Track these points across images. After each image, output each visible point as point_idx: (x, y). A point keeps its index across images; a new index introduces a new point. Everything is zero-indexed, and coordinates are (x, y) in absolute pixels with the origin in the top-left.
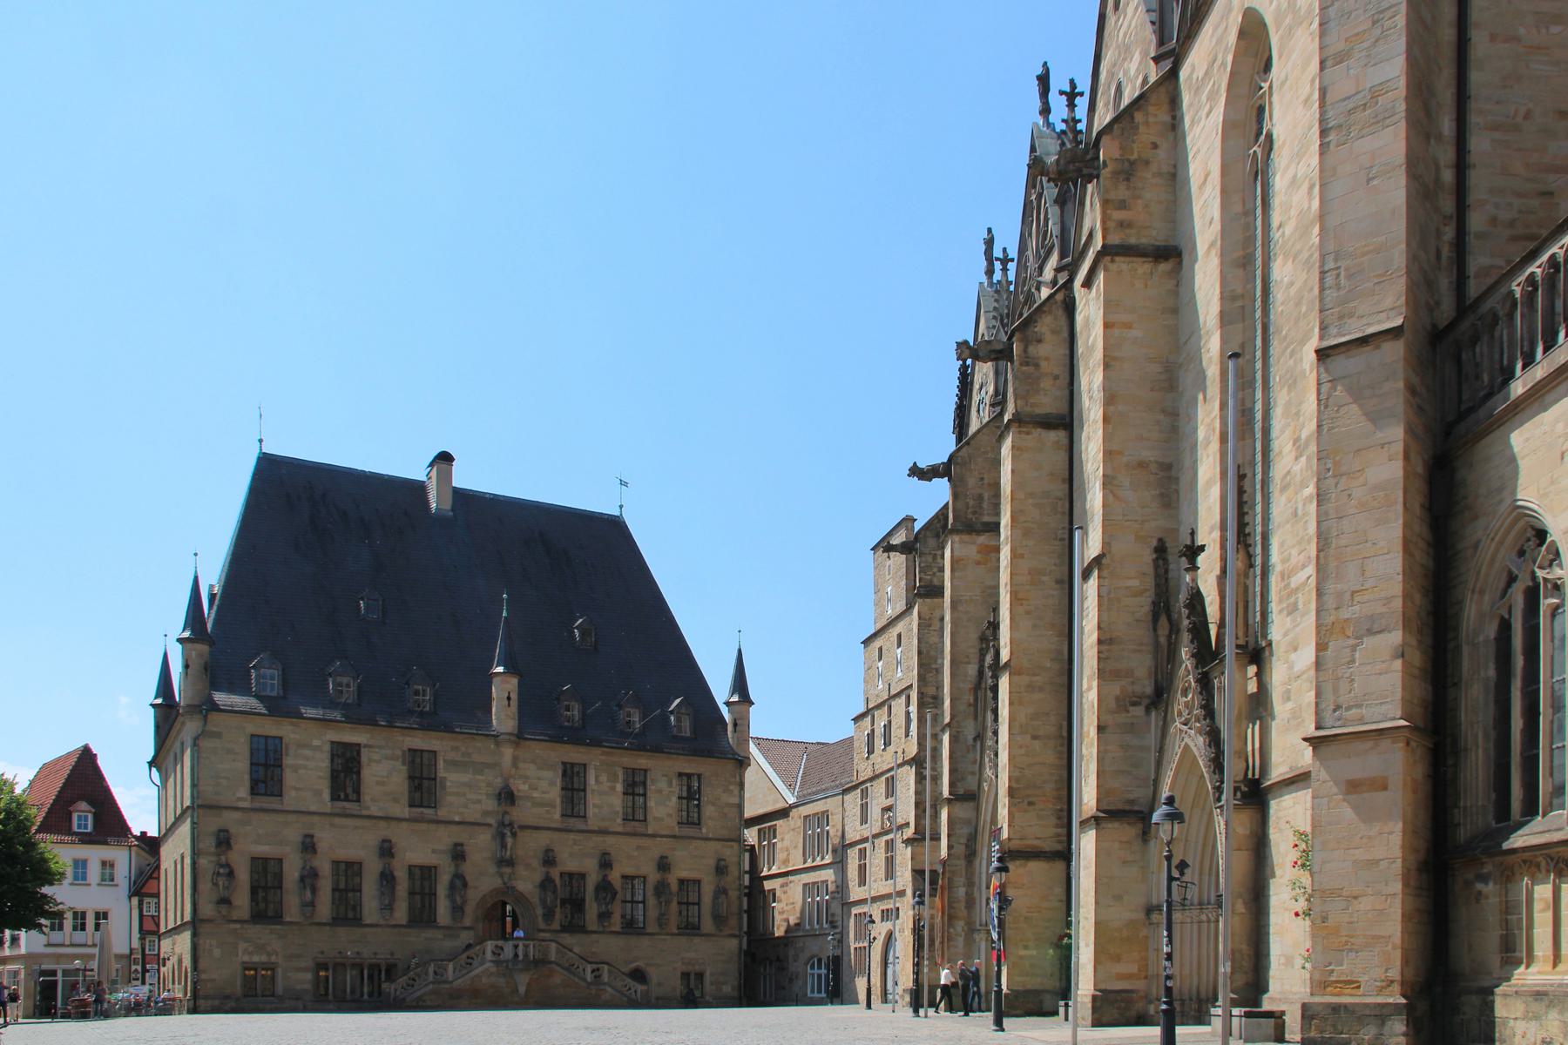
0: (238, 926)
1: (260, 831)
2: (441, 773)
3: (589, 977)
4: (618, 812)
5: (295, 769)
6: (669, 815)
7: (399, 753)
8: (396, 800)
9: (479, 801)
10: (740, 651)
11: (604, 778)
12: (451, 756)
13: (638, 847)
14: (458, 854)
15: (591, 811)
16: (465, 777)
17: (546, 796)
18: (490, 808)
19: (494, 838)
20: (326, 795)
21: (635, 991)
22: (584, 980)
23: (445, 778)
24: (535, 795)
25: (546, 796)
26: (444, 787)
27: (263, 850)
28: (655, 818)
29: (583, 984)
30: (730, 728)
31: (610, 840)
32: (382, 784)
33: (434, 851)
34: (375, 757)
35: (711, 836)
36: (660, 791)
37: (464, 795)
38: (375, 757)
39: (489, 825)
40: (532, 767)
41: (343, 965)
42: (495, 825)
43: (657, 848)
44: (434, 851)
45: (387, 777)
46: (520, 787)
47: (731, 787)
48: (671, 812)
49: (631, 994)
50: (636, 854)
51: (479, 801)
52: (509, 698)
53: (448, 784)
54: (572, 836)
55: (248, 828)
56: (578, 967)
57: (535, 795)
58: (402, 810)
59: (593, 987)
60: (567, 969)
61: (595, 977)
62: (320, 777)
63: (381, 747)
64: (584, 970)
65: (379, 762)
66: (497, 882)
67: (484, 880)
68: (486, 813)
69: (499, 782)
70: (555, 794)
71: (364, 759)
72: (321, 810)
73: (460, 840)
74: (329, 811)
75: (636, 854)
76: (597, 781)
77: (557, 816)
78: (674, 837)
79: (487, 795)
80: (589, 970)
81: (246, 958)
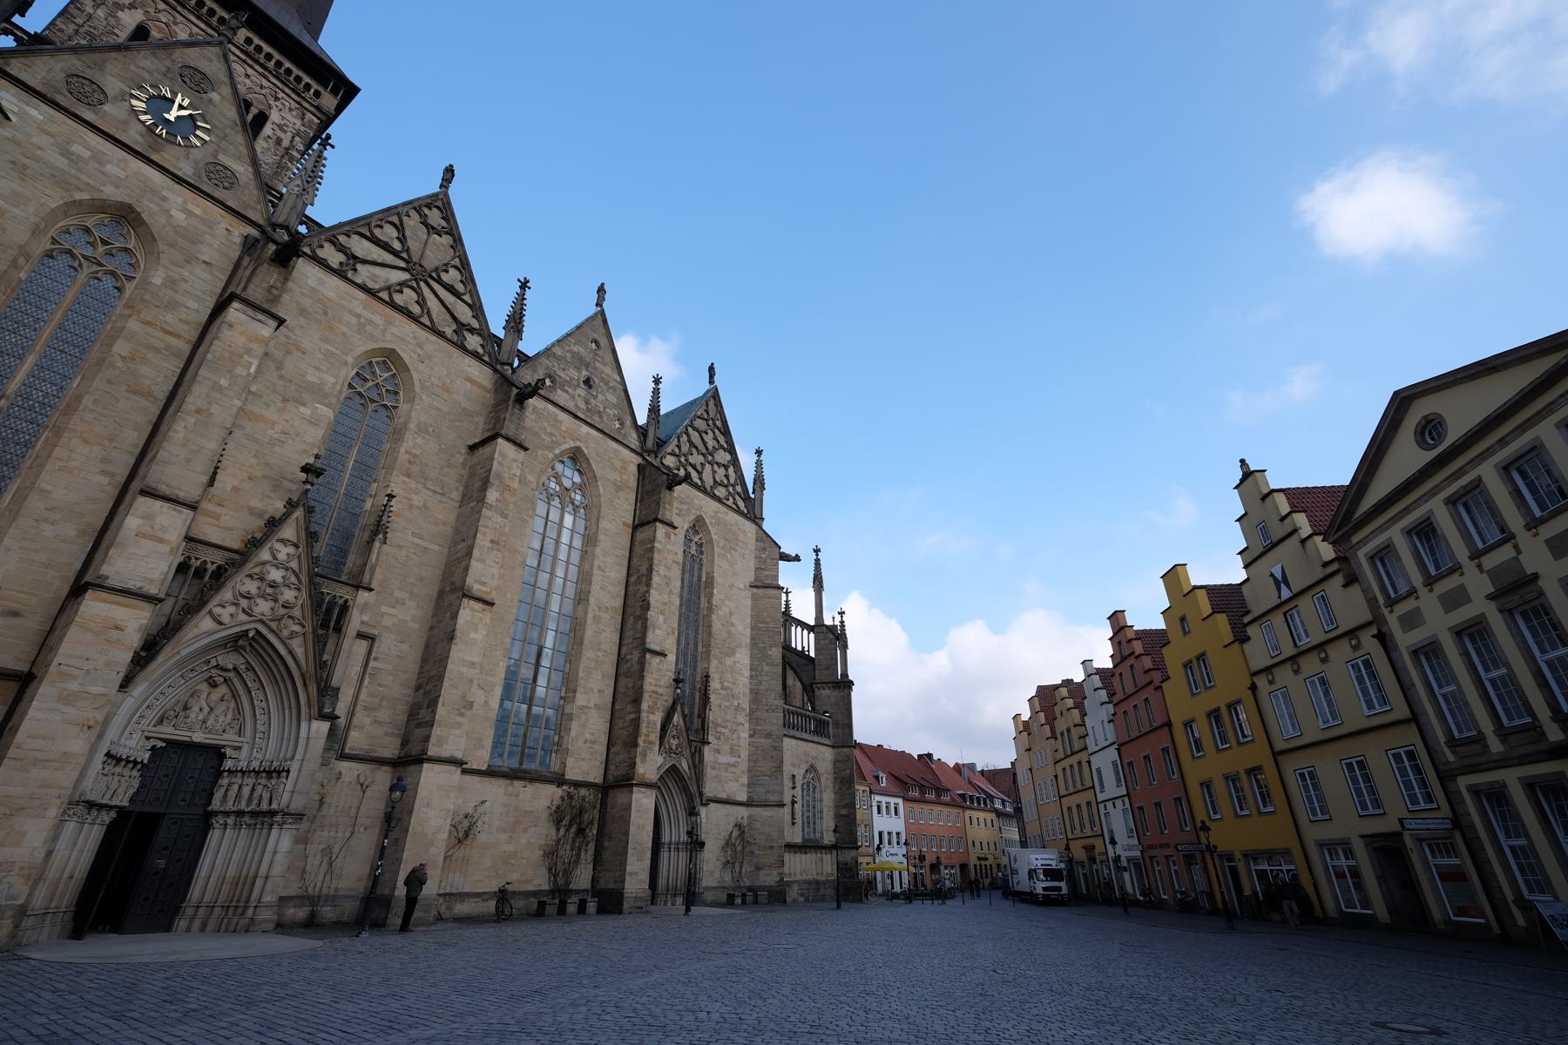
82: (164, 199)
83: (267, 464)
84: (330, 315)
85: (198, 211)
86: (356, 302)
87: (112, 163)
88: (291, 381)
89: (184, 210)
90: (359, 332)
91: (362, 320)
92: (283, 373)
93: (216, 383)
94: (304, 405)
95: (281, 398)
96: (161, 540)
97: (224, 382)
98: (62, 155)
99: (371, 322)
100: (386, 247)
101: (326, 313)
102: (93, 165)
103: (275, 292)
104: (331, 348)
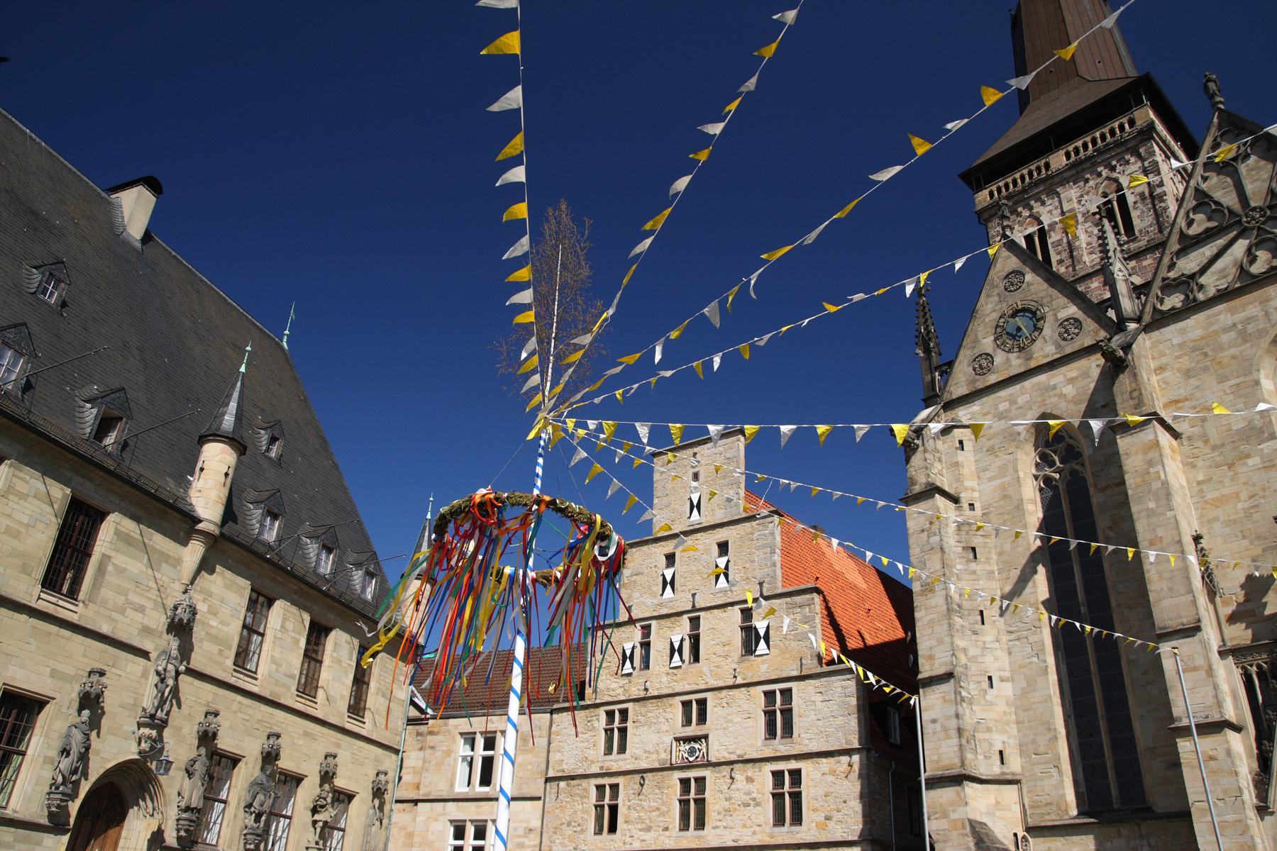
4: (292, 677)
8: (25, 570)
9: (141, 610)
11: (290, 626)
13: (306, 734)
17: (225, 629)
18: (153, 625)
19: (145, 675)
23: (109, 557)
24: (213, 623)
25: (225, 629)
26: (101, 570)
32: (17, 536)
33: (54, 674)
36: (339, 662)
37: (125, 593)
39: (144, 654)
44: (54, 674)
51: (141, 610)
52: (227, 475)
53: (110, 568)
65: (23, 496)
66: (130, 752)
68: (146, 631)
73: (99, 666)
75: (301, 742)
82: (1054, 387)
83: (1258, 538)
84: (1210, 353)
85: (1074, 374)
86: (1222, 317)
87: (1018, 396)
88: (1223, 445)
89: (1071, 381)
90: (1245, 341)
91: (1240, 327)
92: (1212, 442)
93: (1148, 509)
94: (1248, 456)
95: (1226, 467)
96: (1195, 669)
97: (1152, 505)
98: (999, 419)
99: (1249, 320)
100: (1207, 236)
101: (1206, 355)
102: (1015, 407)
103: (1135, 394)
104: (1233, 382)
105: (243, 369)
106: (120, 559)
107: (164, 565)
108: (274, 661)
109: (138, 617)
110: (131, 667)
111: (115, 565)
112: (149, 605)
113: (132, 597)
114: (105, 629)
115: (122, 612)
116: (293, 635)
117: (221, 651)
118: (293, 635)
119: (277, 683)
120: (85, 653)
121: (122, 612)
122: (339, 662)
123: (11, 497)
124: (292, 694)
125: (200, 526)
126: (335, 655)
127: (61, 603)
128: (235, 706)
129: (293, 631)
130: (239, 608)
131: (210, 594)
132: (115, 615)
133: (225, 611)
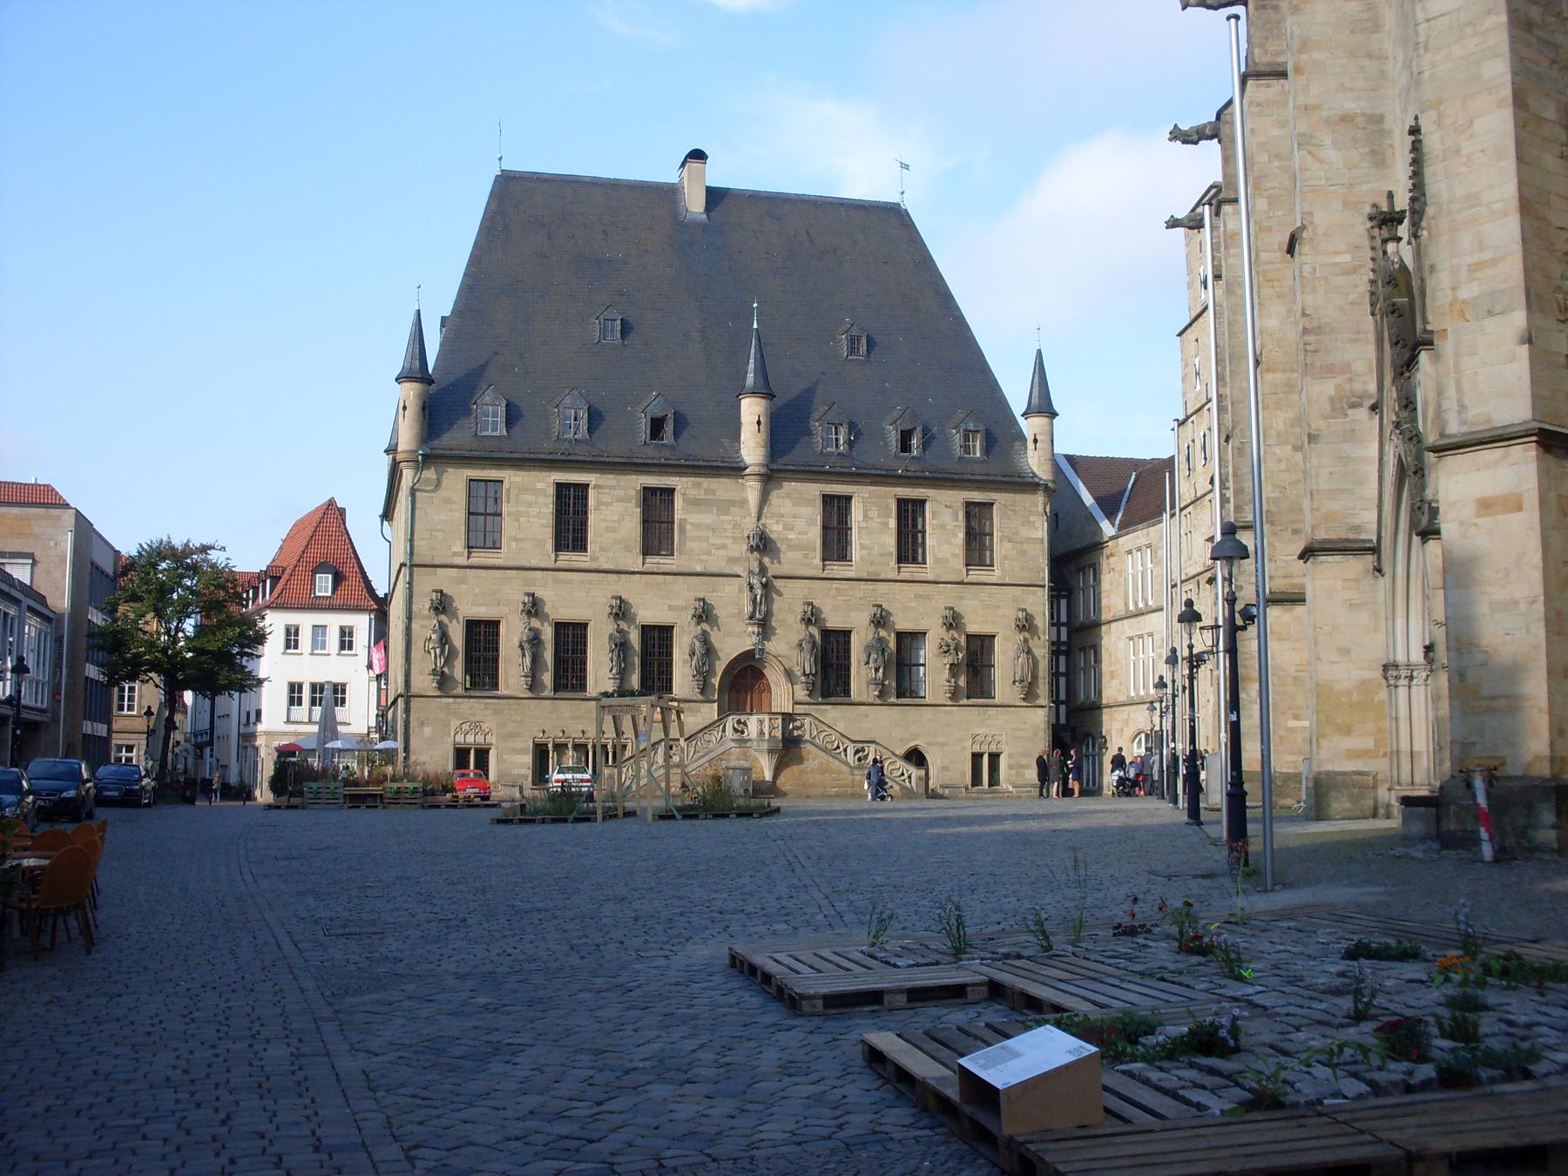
0: (451, 700)
1: (477, 591)
2: (679, 514)
3: (851, 758)
5: (517, 516)
6: (954, 555)
7: (633, 493)
8: (628, 549)
9: (724, 546)
10: (1039, 352)
11: (873, 513)
12: (693, 493)
13: (916, 596)
14: (705, 614)
15: (856, 552)
16: (708, 518)
18: (737, 554)
19: (741, 590)
20: (549, 545)
21: (910, 777)
22: (846, 763)
23: (685, 520)
25: (805, 537)
26: (683, 531)
27: (482, 612)
28: (937, 560)
29: (844, 768)
30: (1030, 445)
31: (882, 588)
32: (614, 530)
33: (670, 608)
34: (606, 498)
35: (1007, 581)
36: (943, 527)
38: (606, 498)
40: (788, 503)
41: (566, 746)
42: (745, 574)
43: (943, 598)
44: (670, 608)
45: (619, 522)
46: (775, 529)
47: (1032, 519)
48: (957, 551)
49: (904, 781)
50: (913, 604)
51: (724, 546)
52: (759, 423)
53: (688, 527)
54: (835, 584)
55: (464, 587)
56: (838, 747)
57: (789, 536)
58: (634, 561)
59: (856, 772)
60: (825, 750)
61: (860, 759)
62: (543, 526)
63: (611, 488)
64: (845, 750)
67: (734, 641)
68: (732, 560)
69: (749, 525)
70: (814, 534)
71: (591, 502)
72: (542, 565)
74: (551, 565)
75: (913, 604)
76: (865, 516)
77: (818, 561)
78: (962, 583)
79: (734, 538)
80: (850, 752)
81: (460, 738)
105: (755, 326)
106: (694, 518)
107: (732, 509)
108: (862, 547)
109: (723, 552)
110: (727, 589)
111: (692, 524)
112: (729, 542)
113: (712, 541)
114: (699, 569)
115: (708, 553)
116: (879, 520)
117: (806, 556)
118: (879, 520)
119: (872, 563)
120: (699, 587)
121: (708, 553)
122: (943, 527)
123: (601, 507)
124: (892, 568)
125: (747, 471)
126: (935, 522)
127: (661, 561)
128: (833, 592)
129: (879, 516)
130: (814, 517)
131: (782, 516)
132: (703, 557)
133: (801, 524)
